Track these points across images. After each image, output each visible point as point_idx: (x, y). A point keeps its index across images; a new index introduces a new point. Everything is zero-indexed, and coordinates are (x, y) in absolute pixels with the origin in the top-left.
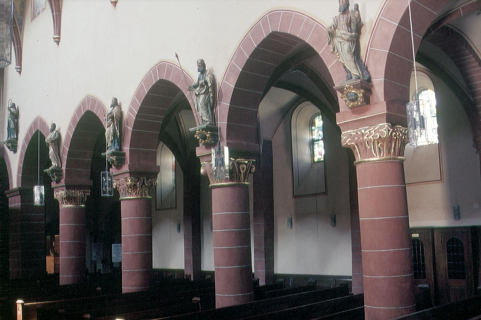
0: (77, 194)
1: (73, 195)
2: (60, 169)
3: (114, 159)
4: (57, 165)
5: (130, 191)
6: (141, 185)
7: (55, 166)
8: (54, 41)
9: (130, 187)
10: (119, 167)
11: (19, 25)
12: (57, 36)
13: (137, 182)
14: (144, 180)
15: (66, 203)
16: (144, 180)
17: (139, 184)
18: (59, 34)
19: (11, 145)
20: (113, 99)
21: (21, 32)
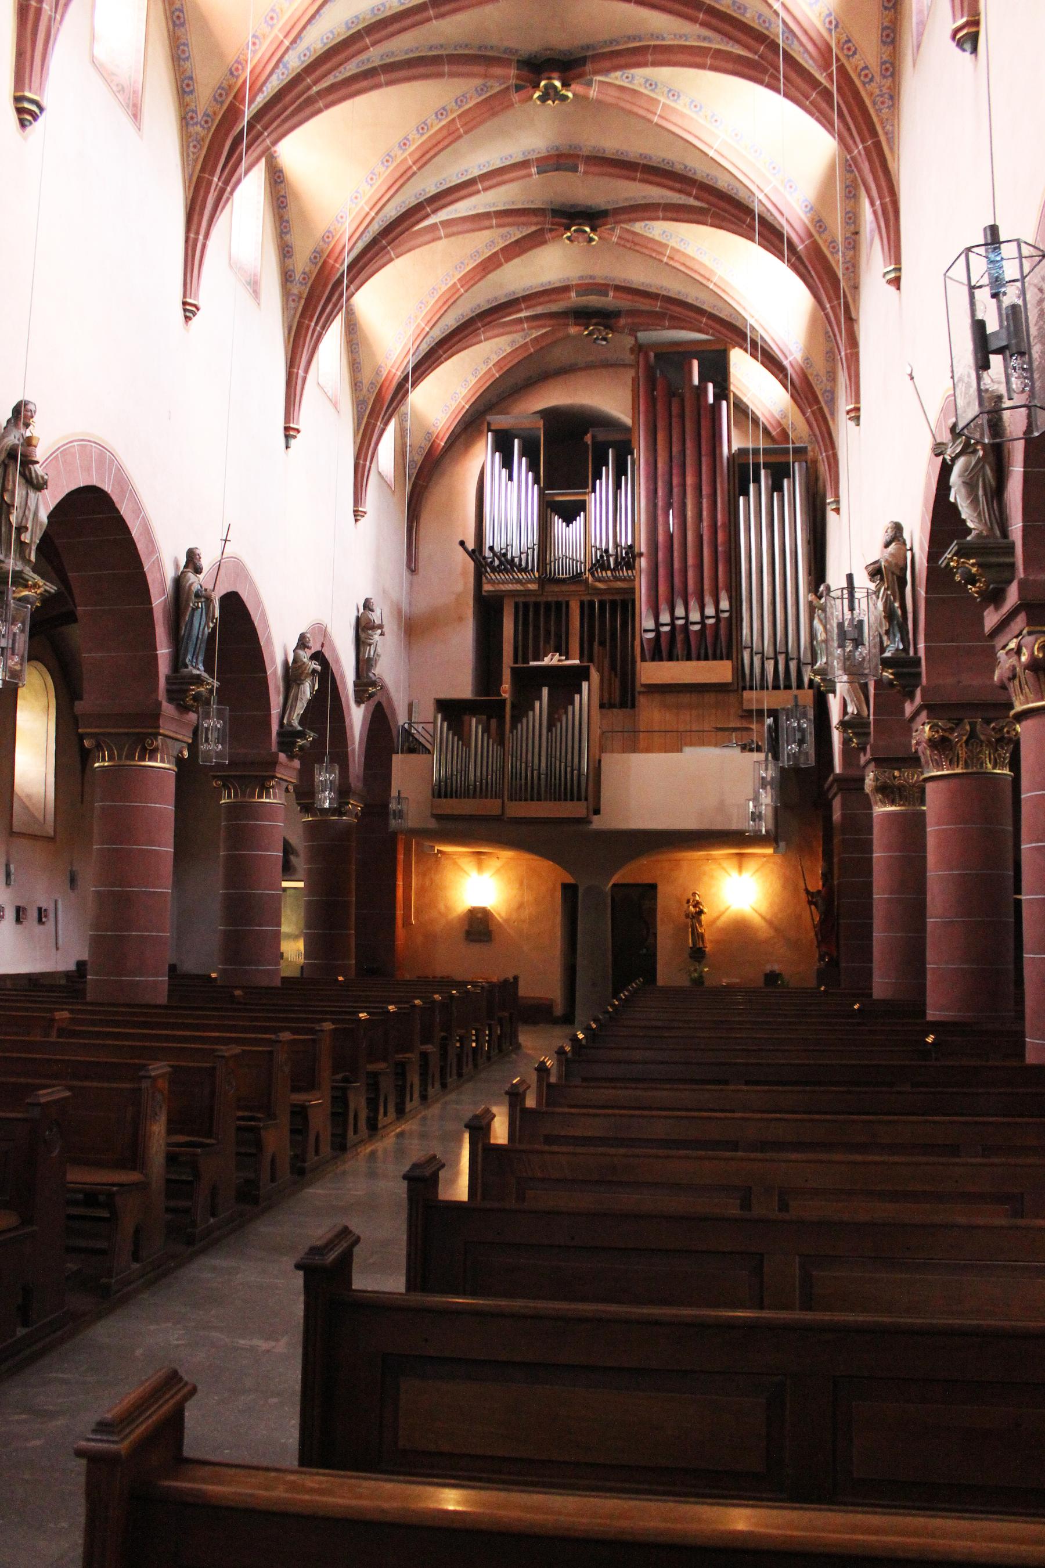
0: (905, 781)
1: (897, 782)
2: (865, 721)
3: (891, 677)
4: (855, 712)
5: (936, 757)
6: (965, 738)
7: (853, 714)
8: (849, 419)
9: (932, 743)
10: (911, 696)
11: (826, 402)
12: (852, 406)
13: (952, 730)
14: (973, 725)
15: (884, 804)
16: (973, 725)
17: (957, 737)
18: (857, 399)
19: (821, 679)
20: (890, 525)
21: (833, 419)
